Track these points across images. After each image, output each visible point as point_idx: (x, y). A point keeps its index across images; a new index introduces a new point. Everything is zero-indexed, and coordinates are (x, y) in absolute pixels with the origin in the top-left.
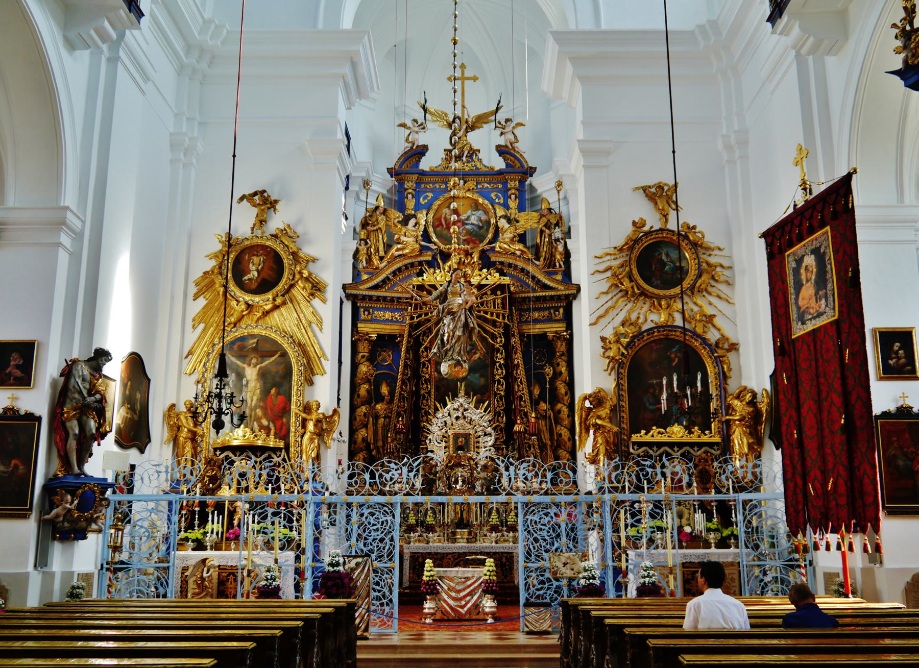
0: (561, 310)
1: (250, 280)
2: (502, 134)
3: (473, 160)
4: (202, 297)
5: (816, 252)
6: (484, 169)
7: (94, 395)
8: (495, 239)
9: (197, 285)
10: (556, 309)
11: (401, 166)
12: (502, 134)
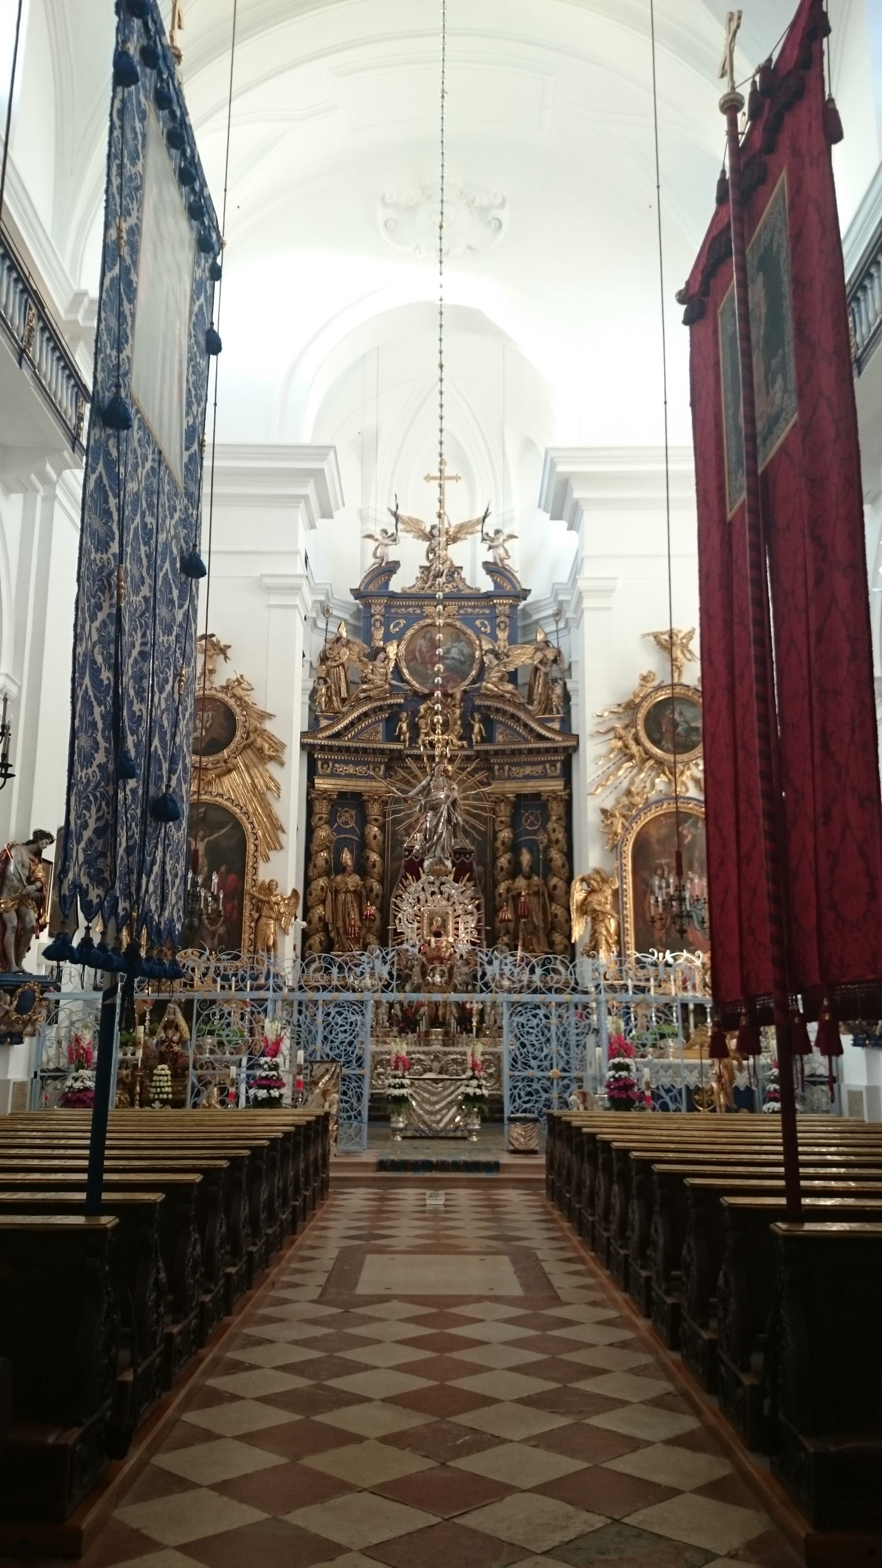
0: (559, 765)
2: (490, 548)
3: (454, 580)
6: (468, 591)
7: (33, 883)
8: (479, 677)
10: (553, 764)
11: (366, 587)
12: (490, 548)
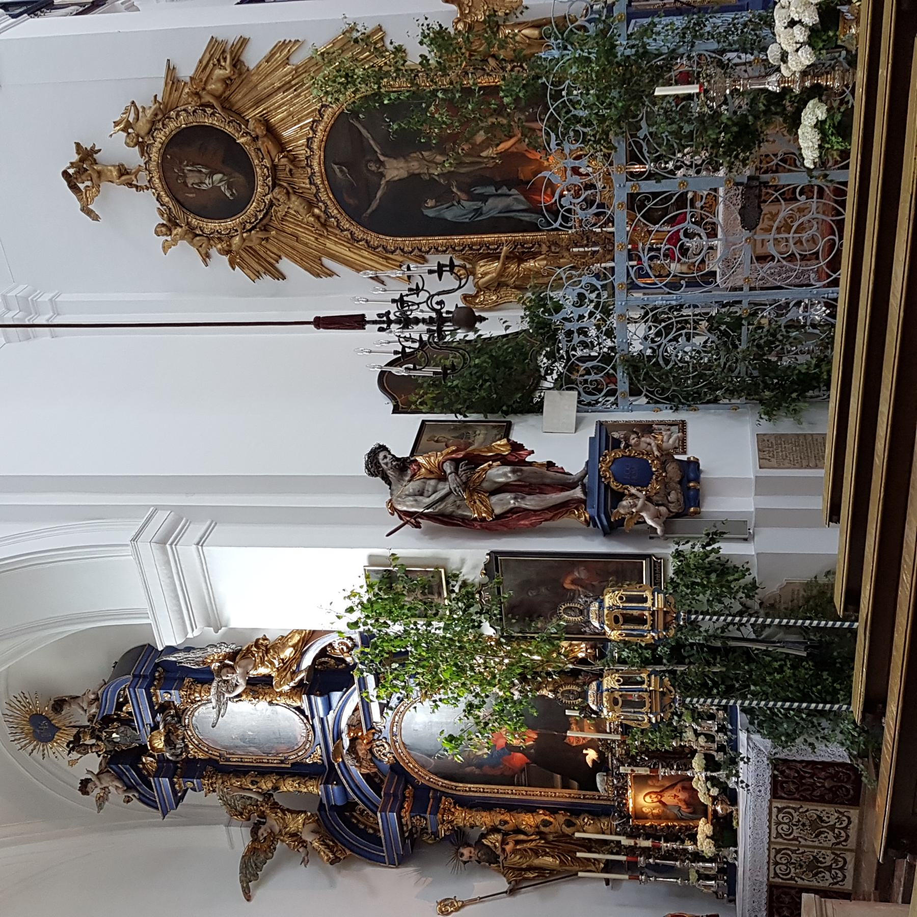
1: (230, 188)
4: (277, 265)
9: (258, 275)
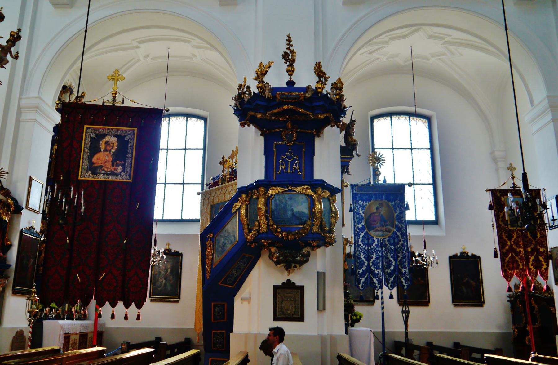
5: (120, 138)
